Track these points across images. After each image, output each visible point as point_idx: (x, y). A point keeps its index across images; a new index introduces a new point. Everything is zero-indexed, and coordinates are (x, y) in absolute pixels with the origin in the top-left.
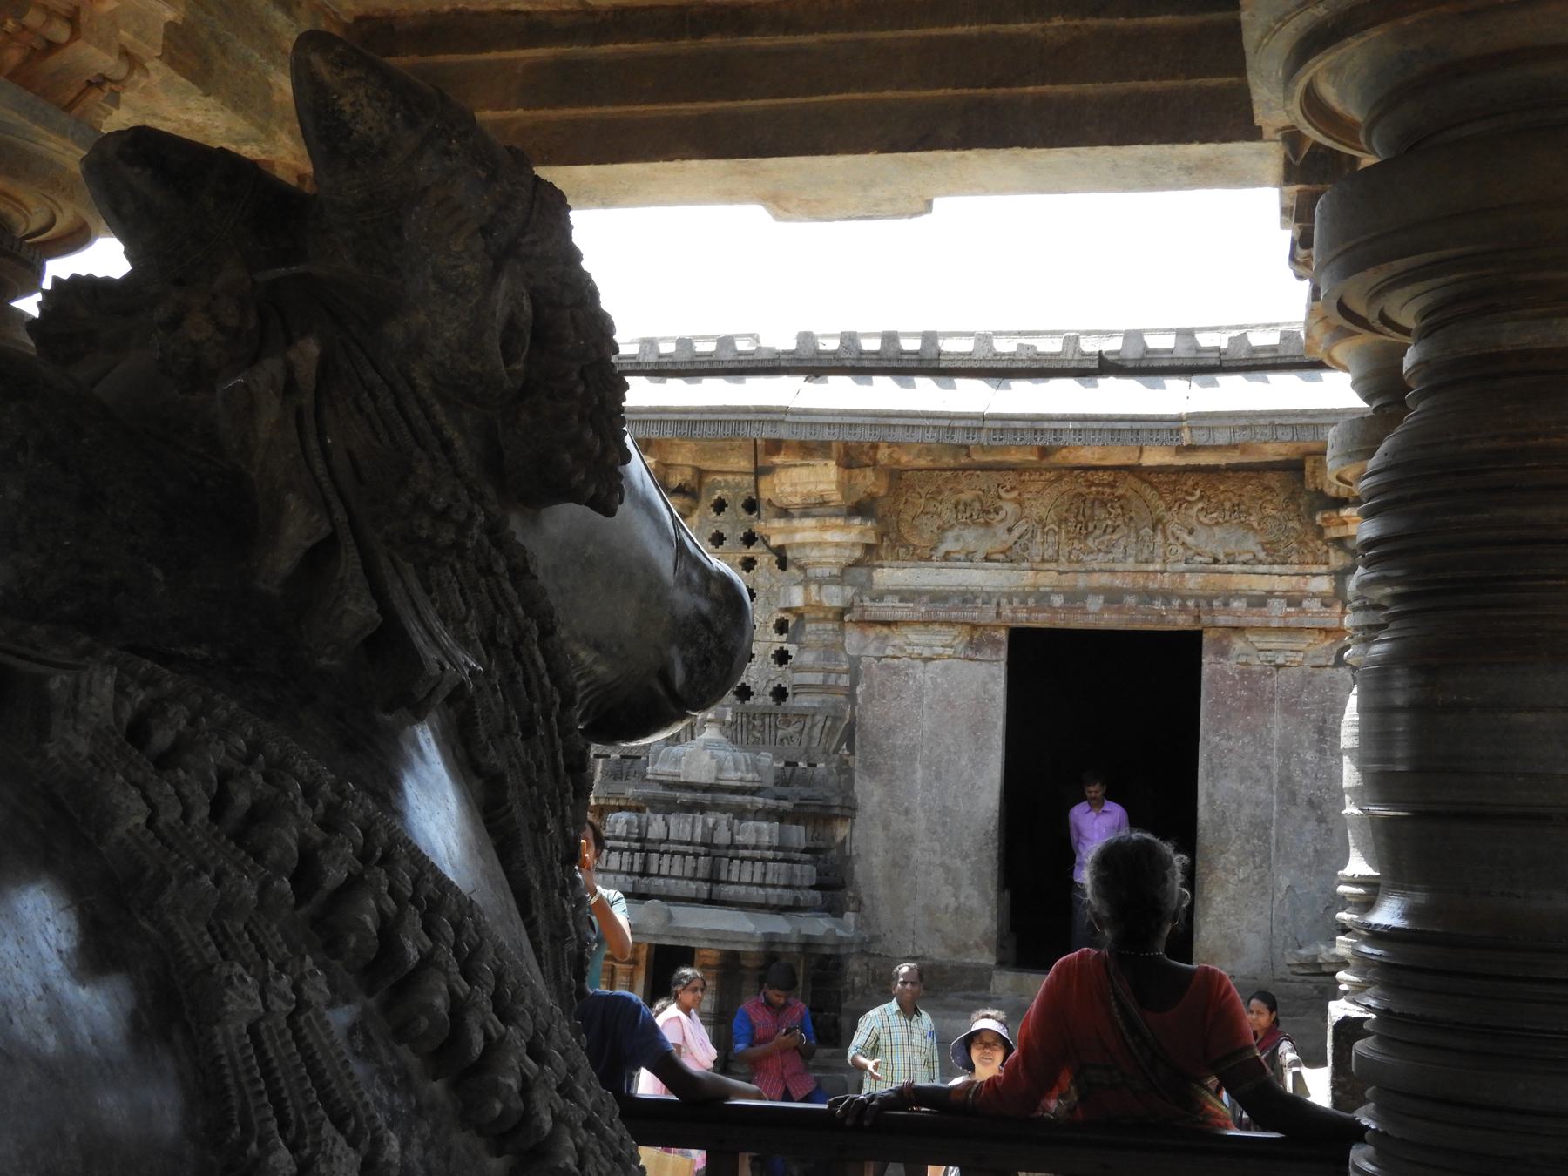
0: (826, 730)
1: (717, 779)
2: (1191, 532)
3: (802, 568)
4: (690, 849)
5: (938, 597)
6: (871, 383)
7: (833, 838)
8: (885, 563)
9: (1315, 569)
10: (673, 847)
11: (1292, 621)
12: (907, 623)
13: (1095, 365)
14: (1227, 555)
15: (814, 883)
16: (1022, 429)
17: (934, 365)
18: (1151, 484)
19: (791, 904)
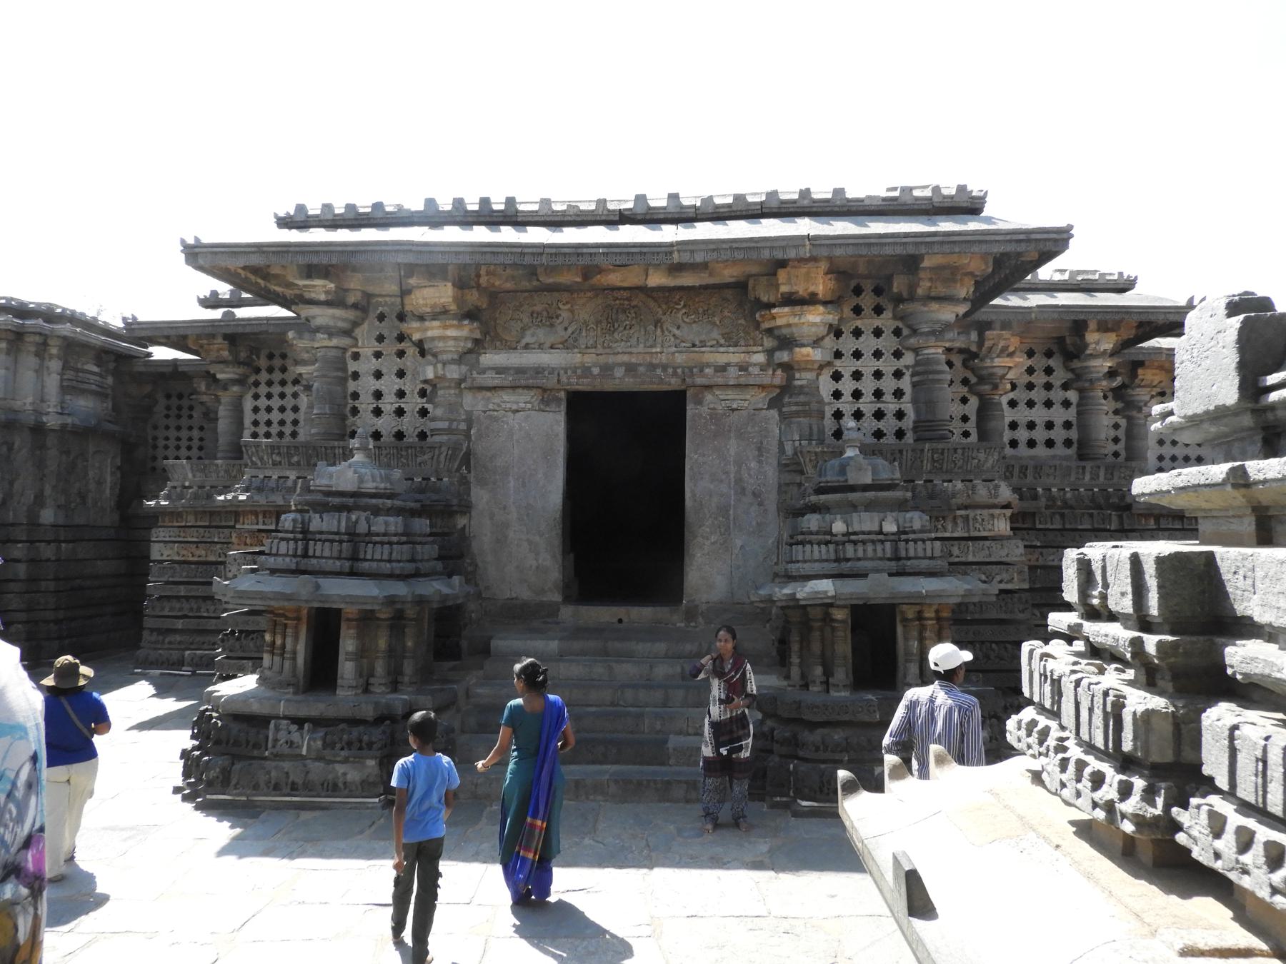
0: (448, 456)
1: (359, 488)
2: (678, 328)
3: (435, 355)
4: (337, 537)
5: (520, 371)
6: (472, 229)
7: (455, 526)
8: (488, 351)
9: (755, 349)
10: (324, 537)
11: (743, 381)
12: (502, 388)
13: (617, 218)
14: (701, 342)
15: (437, 556)
16: (569, 254)
17: (514, 219)
18: (653, 298)
19: (413, 572)
